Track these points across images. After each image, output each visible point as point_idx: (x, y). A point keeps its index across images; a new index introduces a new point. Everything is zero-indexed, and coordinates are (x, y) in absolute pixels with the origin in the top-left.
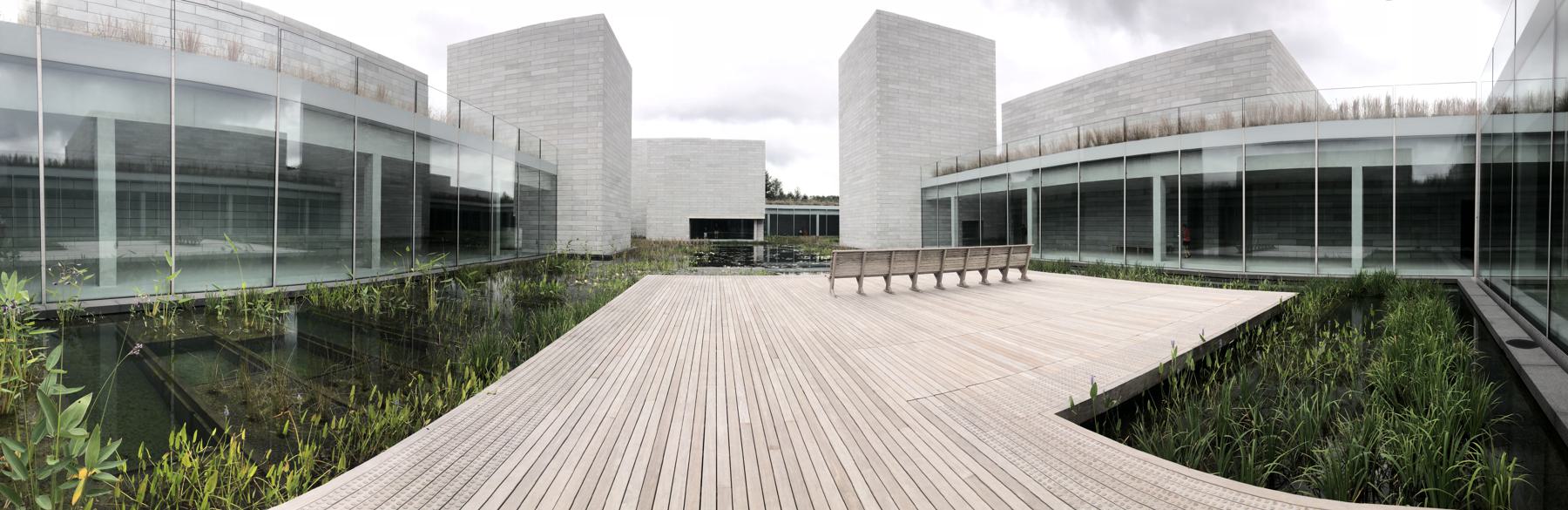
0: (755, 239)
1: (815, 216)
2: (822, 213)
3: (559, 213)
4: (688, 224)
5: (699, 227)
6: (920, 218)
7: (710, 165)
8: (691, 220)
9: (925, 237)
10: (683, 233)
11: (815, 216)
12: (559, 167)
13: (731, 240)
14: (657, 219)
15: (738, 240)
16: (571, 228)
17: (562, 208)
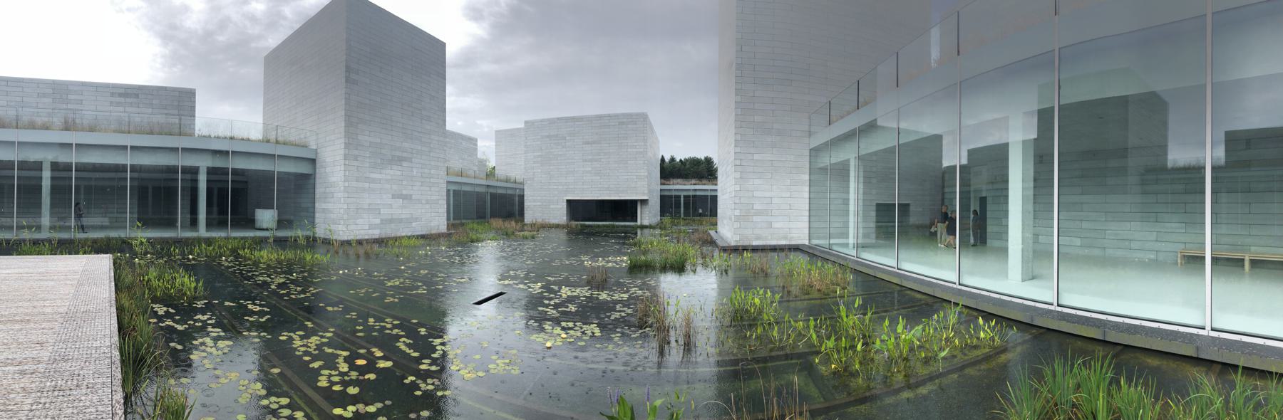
0: (639, 223)
1: (680, 197)
2: (686, 193)
3: (317, 196)
4: (565, 204)
5: (577, 209)
6: (807, 195)
7: (588, 143)
8: (568, 201)
9: (812, 225)
10: (559, 214)
11: (680, 197)
12: (319, 151)
13: (608, 223)
14: (534, 201)
15: (617, 223)
16: (324, 211)
17: (319, 190)
